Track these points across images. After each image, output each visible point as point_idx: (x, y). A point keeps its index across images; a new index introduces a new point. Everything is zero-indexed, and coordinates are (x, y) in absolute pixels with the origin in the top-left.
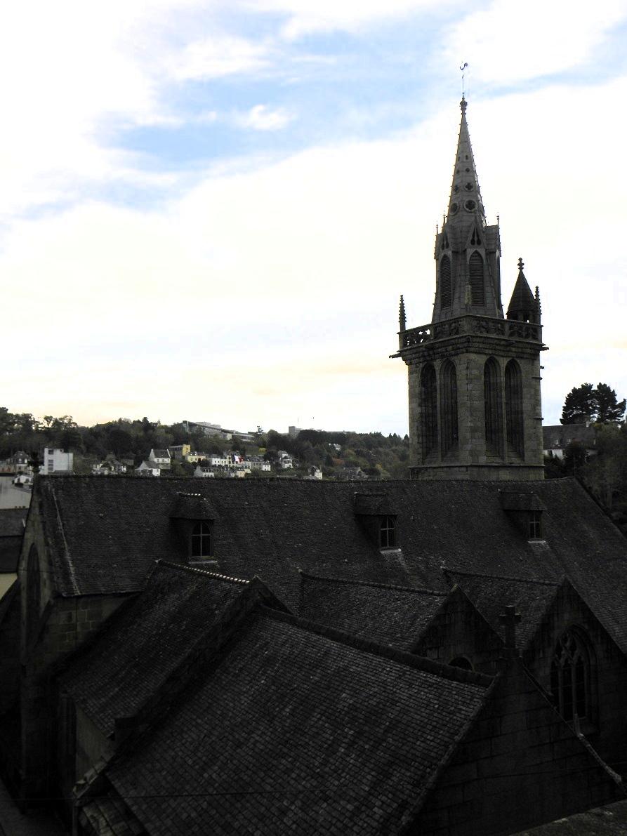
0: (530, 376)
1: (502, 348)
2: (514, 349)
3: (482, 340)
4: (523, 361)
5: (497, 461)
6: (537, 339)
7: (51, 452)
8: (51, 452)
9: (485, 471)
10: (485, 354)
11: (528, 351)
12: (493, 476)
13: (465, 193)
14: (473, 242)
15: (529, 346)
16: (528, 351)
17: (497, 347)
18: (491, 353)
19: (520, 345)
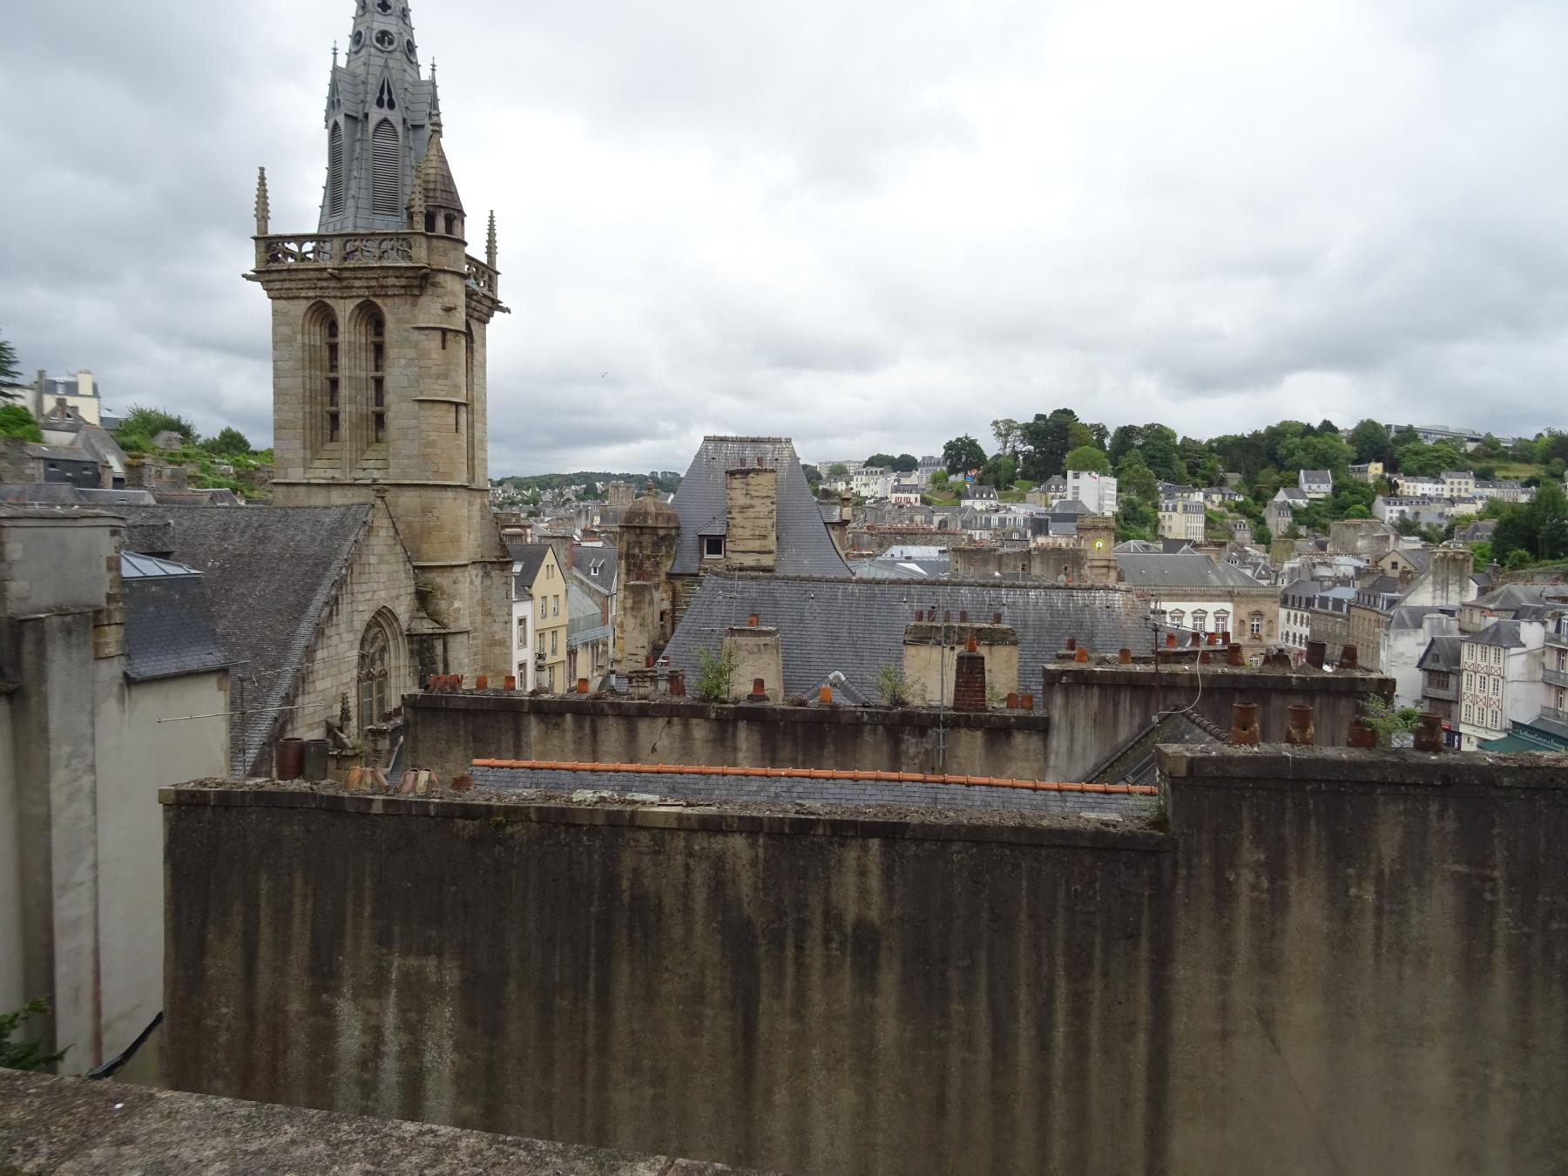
0: (408, 326)
1: (333, 284)
2: (358, 283)
3: (284, 275)
4: (389, 301)
5: (320, 473)
6: (410, 258)
7: (1076, 477)
8: (1076, 477)
9: (302, 490)
10: (307, 298)
11: (391, 281)
12: (318, 498)
13: (377, 17)
14: (380, 103)
15: (391, 272)
16: (391, 281)
17: (320, 284)
18: (311, 293)
19: (370, 274)
